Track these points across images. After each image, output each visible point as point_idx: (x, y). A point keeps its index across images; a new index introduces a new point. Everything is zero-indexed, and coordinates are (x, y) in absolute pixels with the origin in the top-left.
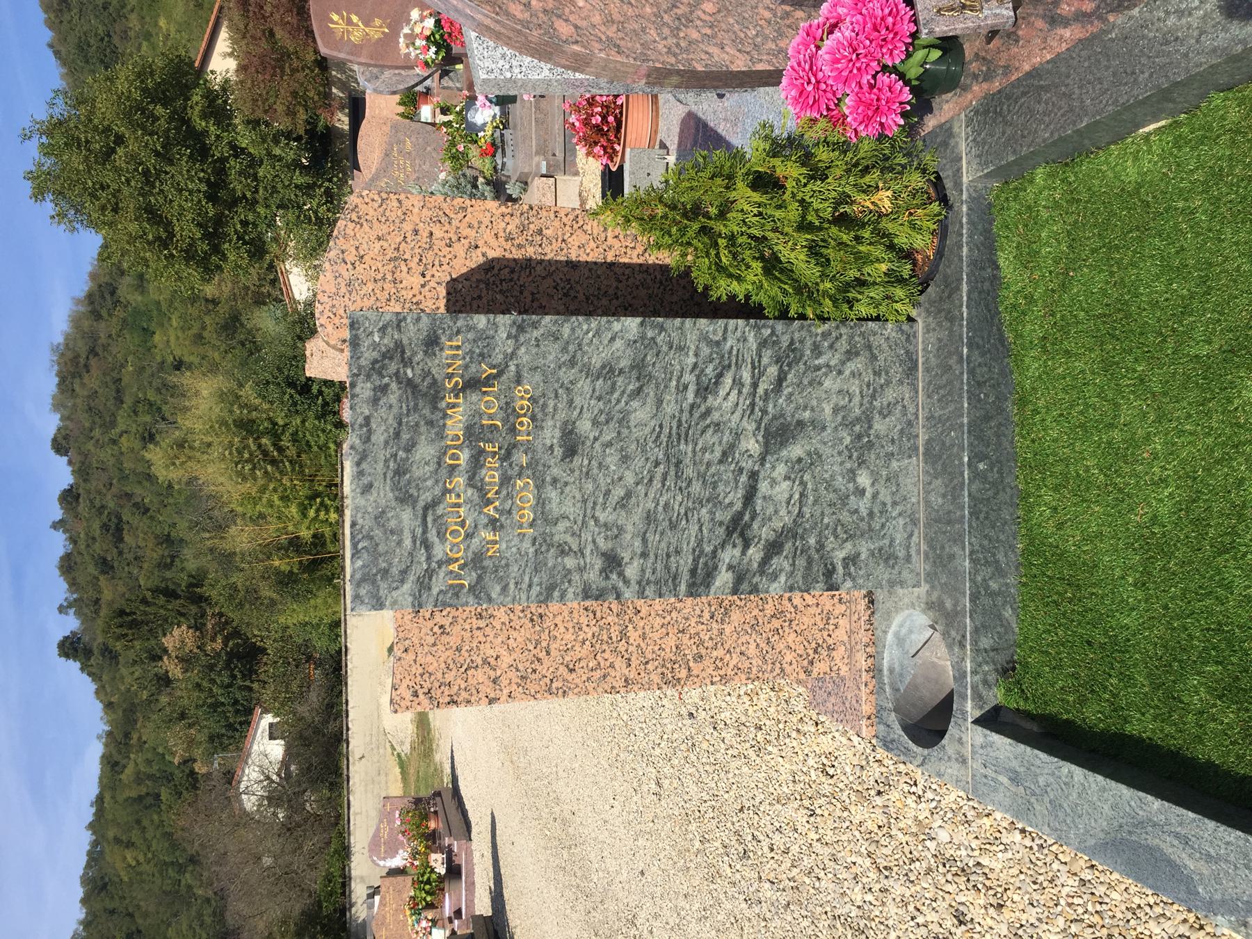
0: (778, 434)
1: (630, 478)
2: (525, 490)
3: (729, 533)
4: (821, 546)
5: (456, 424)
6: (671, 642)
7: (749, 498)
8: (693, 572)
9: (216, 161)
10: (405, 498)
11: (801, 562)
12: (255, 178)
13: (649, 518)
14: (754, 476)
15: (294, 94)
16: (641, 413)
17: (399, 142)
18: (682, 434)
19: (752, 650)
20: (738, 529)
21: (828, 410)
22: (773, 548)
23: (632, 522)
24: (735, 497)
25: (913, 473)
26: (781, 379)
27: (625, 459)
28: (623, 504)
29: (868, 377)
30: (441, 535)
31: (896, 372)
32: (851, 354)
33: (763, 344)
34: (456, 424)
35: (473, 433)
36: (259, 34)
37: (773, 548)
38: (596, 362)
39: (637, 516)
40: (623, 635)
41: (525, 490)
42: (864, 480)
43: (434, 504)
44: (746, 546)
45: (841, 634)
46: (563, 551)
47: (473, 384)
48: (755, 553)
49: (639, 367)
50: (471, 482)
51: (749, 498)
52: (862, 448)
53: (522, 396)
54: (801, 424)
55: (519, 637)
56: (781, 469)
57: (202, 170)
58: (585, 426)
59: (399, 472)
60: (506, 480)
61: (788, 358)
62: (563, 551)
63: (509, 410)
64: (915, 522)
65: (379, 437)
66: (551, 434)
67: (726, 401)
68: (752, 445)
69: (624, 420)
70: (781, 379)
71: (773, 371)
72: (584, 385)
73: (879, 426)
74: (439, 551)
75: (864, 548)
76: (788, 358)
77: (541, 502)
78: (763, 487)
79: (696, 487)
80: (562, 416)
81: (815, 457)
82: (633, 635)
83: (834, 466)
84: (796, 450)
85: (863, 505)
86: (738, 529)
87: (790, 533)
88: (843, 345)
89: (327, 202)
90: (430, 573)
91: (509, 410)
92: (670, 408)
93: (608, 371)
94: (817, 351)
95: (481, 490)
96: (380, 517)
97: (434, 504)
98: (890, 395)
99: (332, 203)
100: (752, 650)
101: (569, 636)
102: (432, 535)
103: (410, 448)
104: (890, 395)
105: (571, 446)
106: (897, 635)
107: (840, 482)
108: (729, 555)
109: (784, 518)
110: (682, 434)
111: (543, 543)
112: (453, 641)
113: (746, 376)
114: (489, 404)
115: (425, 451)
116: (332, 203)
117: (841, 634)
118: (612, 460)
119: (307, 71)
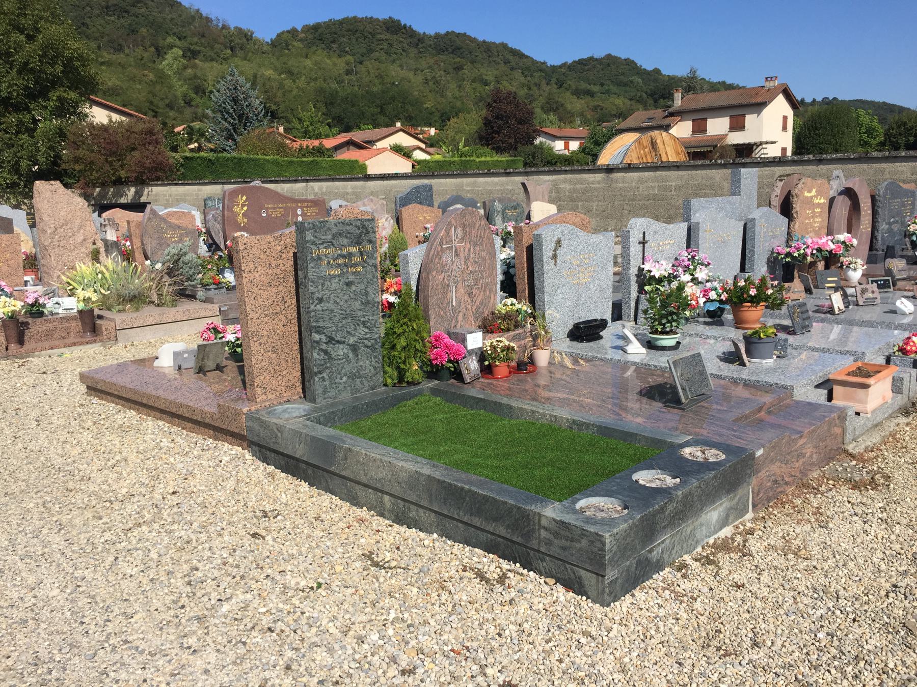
0: (354, 348)
1: (342, 303)
2: (337, 272)
3: (329, 337)
4: (327, 368)
5: (353, 250)
6: (265, 333)
7: (339, 342)
8: (319, 327)
9: (26, 104)
10: (334, 236)
11: (322, 362)
12: (18, 132)
13: (332, 311)
14: (344, 342)
15: (91, 163)
16: (357, 305)
17: (186, 233)
18: (353, 318)
19: (264, 364)
20: (331, 340)
21: (361, 363)
22: (326, 352)
23: (330, 306)
24: (338, 338)
25: (346, 396)
26: (367, 347)
27: (346, 301)
28: (336, 302)
29: (370, 375)
30: (325, 248)
31: (371, 384)
32: (375, 368)
33: (376, 340)
34: (353, 250)
35: (350, 255)
36: (132, 141)
37: (326, 352)
38: (369, 290)
39: (333, 307)
40: (266, 315)
41: (337, 272)
42: (345, 379)
43: (333, 245)
44: (326, 343)
45: (270, 396)
46: (323, 285)
47: (361, 254)
48: (324, 347)
49: (368, 302)
50: (339, 255)
51: (339, 342)
52: (352, 377)
53: (360, 269)
54: (357, 355)
55: (264, 278)
56: (346, 351)
57: (18, 95)
58: (353, 288)
59: (340, 234)
60: (339, 265)
61: (373, 348)
62: (323, 285)
63: (356, 265)
64: (334, 398)
65: (348, 228)
66: (351, 278)
67: (362, 330)
68: (352, 340)
69: (356, 300)
70: (367, 347)
71: (370, 344)
72: (363, 286)
73: (358, 381)
74: (321, 247)
75: (327, 383)
76: (373, 348)
77: (334, 276)
78: (341, 346)
79: (340, 325)
80: (356, 281)
81: (349, 361)
82: (266, 319)
83: (348, 368)
84: (351, 355)
85: (338, 380)
86: (331, 340)
87: (330, 358)
88: (377, 365)
89: (7, 184)
90: (316, 245)
91: (356, 265)
92: (360, 313)
93: (367, 293)
94: (375, 357)
95: (337, 258)
96: (329, 229)
97: (333, 245)
98: (366, 383)
99: (7, 187)
100: (264, 364)
101: (265, 296)
102: (325, 245)
103: (346, 237)
104: (366, 383)
105: (349, 284)
106: (288, 408)
107: (344, 371)
108: (323, 338)
109: (334, 355)
110: (353, 318)
111: (324, 278)
112: (262, 256)
113: (368, 336)
114: (358, 259)
115: (345, 241)
116: (7, 187)
117: (270, 396)
118: (346, 297)
119: (112, 172)
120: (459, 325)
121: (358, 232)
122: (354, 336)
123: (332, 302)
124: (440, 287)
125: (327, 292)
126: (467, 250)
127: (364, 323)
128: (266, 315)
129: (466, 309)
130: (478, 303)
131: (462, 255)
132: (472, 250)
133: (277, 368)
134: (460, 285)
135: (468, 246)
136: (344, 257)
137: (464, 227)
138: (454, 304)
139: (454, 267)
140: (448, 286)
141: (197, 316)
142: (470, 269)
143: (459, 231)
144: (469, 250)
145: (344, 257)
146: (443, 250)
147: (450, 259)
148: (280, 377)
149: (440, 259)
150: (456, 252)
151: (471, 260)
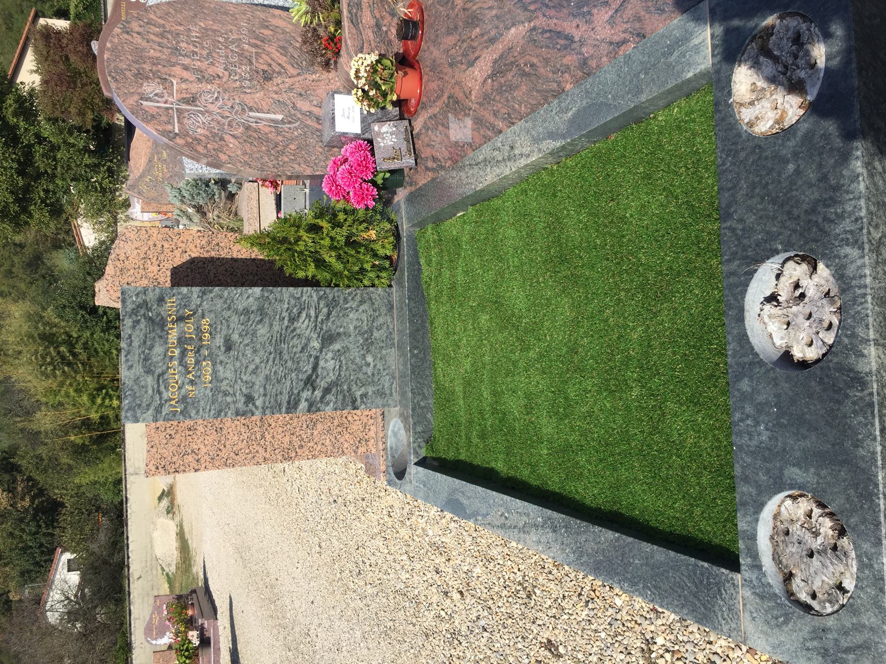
0: (328, 339)
1: (257, 360)
2: (207, 366)
3: (306, 384)
4: (349, 390)
5: (173, 336)
6: (287, 439)
7: (315, 368)
8: (289, 402)
9: (25, 147)
10: (149, 372)
11: (340, 397)
12: (55, 159)
13: (267, 378)
14: (317, 358)
15: (84, 101)
16: (262, 330)
17: (158, 153)
18: (282, 339)
19: (328, 442)
20: (310, 382)
21: (352, 327)
22: (327, 391)
23: (259, 380)
24: (308, 368)
25: (393, 357)
26: (329, 314)
27: (255, 351)
28: (254, 372)
29: (370, 312)
30: (166, 388)
31: (384, 310)
32: (362, 302)
33: (320, 298)
34: (173, 336)
35: (182, 341)
36: (57, 58)
37: (327, 391)
38: (240, 308)
39: (261, 377)
40: (263, 437)
41: (207, 366)
42: (369, 359)
43: (163, 373)
44: (314, 390)
45: (372, 434)
46: (226, 394)
47: (181, 319)
48: (318, 393)
49: (261, 309)
50: (181, 364)
51: (315, 368)
52: (368, 344)
53: (205, 323)
54: (339, 334)
55: (209, 439)
56: (330, 355)
57: (14, 153)
58: (235, 337)
59: (146, 359)
60: (197, 362)
61: (332, 304)
62: (226, 394)
63: (199, 330)
64: (394, 378)
65: (136, 344)
66: (219, 341)
67: (303, 325)
68: (316, 344)
69: (254, 334)
70: (329, 314)
71: (325, 310)
72: (235, 318)
73: (376, 334)
74: (165, 396)
75: (370, 390)
76: (332, 304)
77: (215, 372)
78: (322, 363)
79: (289, 364)
80: (224, 332)
81: (346, 350)
82: (268, 437)
83: (355, 353)
84: (337, 346)
85: (369, 371)
86: (310, 382)
87: (335, 383)
88: (358, 298)
89: (109, 176)
90: (161, 405)
91: (199, 330)
92: (276, 328)
93: (246, 312)
94: (346, 301)
95: (186, 367)
96: (137, 380)
97: (163, 373)
98: (381, 320)
99: (113, 177)
100: (328, 442)
101: (236, 438)
102: (162, 388)
103: (151, 348)
104: (381, 320)
105: (229, 346)
106: (393, 431)
107: (358, 360)
108: (306, 394)
109: (332, 377)
110: (282, 339)
111: (216, 391)
112: (176, 442)
113: (312, 313)
114: (189, 328)
115: (158, 349)
116: (113, 177)
117: (372, 434)
118: (249, 352)
119: (94, 85)
120: (316, 110)
121: (143, 324)
122: (309, 340)
123: (254, 378)
124: (247, 147)
125: (237, 387)
126: (186, 74)
127: (292, 320)
128: (263, 437)
129: (291, 89)
130: (283, 60)
131: (195, 88)
132: (186, 61)
133: (336, 423)
134: (248, 99)
135: (177, 70)
136: (184, 353)
137: (141, 76)
138: (280, 117)
139: (213, 108)
140: (248, 128)
141: (256, 210)
142: (220, 70)
143: (150, 88)
144: (186, 68)
145: (184, 353)
146: (184, 134)
147: (201, 119)
148: (350, 418)
149: (199, 141)
150: (187, 101)
151: (204, 65)
